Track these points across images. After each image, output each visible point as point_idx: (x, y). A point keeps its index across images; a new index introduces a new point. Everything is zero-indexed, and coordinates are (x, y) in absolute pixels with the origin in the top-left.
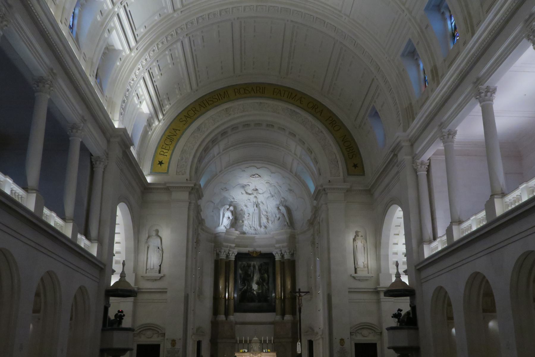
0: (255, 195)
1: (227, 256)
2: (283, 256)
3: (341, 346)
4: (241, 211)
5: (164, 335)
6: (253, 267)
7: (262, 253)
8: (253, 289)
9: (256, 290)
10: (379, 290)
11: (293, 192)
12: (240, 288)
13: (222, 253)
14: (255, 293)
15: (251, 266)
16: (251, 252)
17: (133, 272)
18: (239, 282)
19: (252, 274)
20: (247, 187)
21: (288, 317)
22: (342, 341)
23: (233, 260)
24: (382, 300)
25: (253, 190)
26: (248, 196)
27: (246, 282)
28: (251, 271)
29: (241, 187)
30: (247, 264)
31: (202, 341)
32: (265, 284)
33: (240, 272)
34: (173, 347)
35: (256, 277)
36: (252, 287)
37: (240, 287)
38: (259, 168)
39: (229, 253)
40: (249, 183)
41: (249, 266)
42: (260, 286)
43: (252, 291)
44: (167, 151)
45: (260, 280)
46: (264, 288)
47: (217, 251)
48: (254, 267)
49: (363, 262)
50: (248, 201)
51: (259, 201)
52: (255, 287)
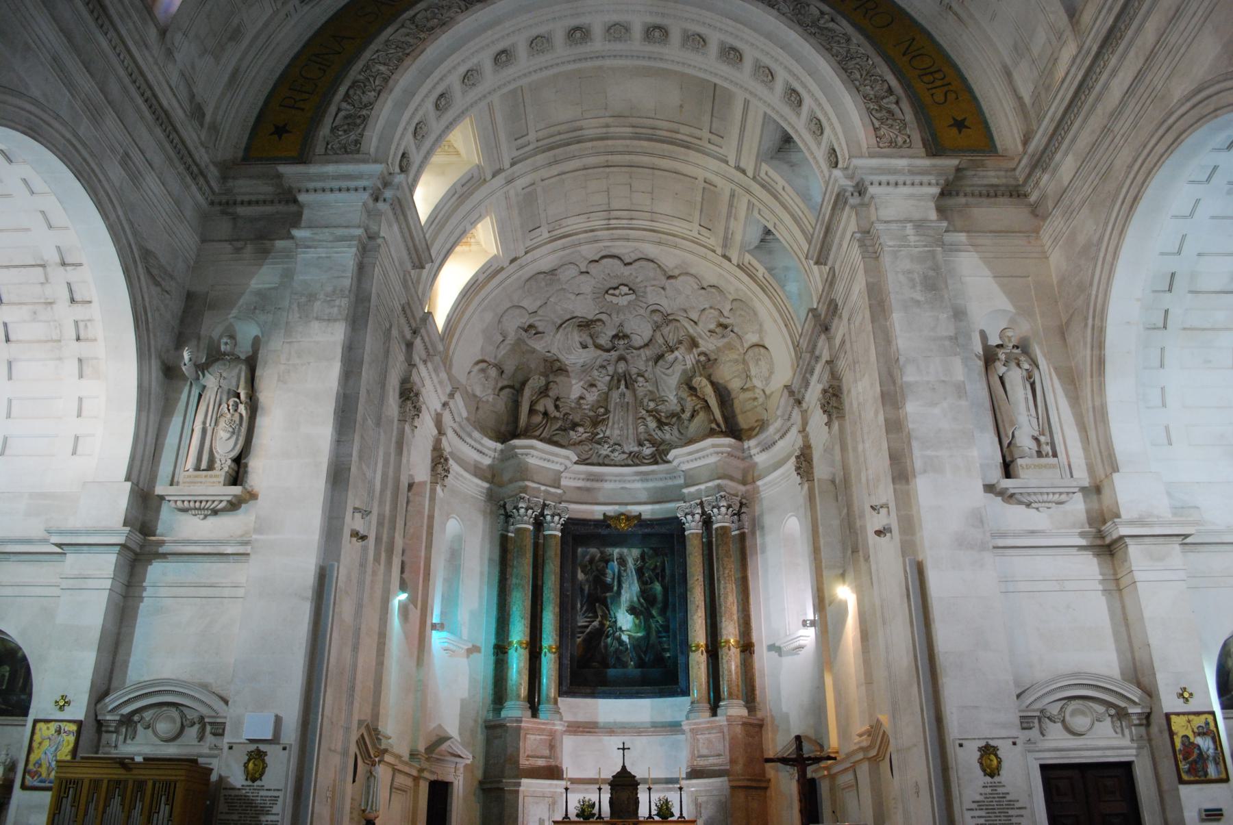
0: (621, 352)
1: (539, 524)
2: (707, 522)
3: (988, 779)
4: (582, 401)
5: (219, 731)
6: (619, 564)
7: (645, 521)
8: (620, 628)
9: (628, 631)
10: (1121, 538)
11: (732, 331)
12: (580, 624)
13: (522, 511)
14: (625, 638)
15: (613, 561)
16: (611, 518)
17: (128, 479)
18: (579, 605)
19: (616, 583)
20: (598, 327)
21: (734, 709)
22: (989, 756)
23: (555, 536)
24: (1138, 576)
25: (616, 336)
26: (599, 352)
27: (597, 604)
28: (614, 575)
29: (579, 326)
30: (602, 553)
31: (452, 783)
32: (654, 612)
33: (581, 576)
34: (254, 780)
35: (630, 591)
36: (615, 622)
37: (581, 622)
38: (630, 264)
39: (542, 514)
40: (603, 317)
41: (606, 560)
42: (642, 617)
43: (618, 634)
44: (306, 96)
45: (639, 600)
46: (653, 625)
47: (507, 506)
48: (622, 561)
49: (1036, 440)
50: (600, 370)
51: (634, 371)
52: (625, 621)
